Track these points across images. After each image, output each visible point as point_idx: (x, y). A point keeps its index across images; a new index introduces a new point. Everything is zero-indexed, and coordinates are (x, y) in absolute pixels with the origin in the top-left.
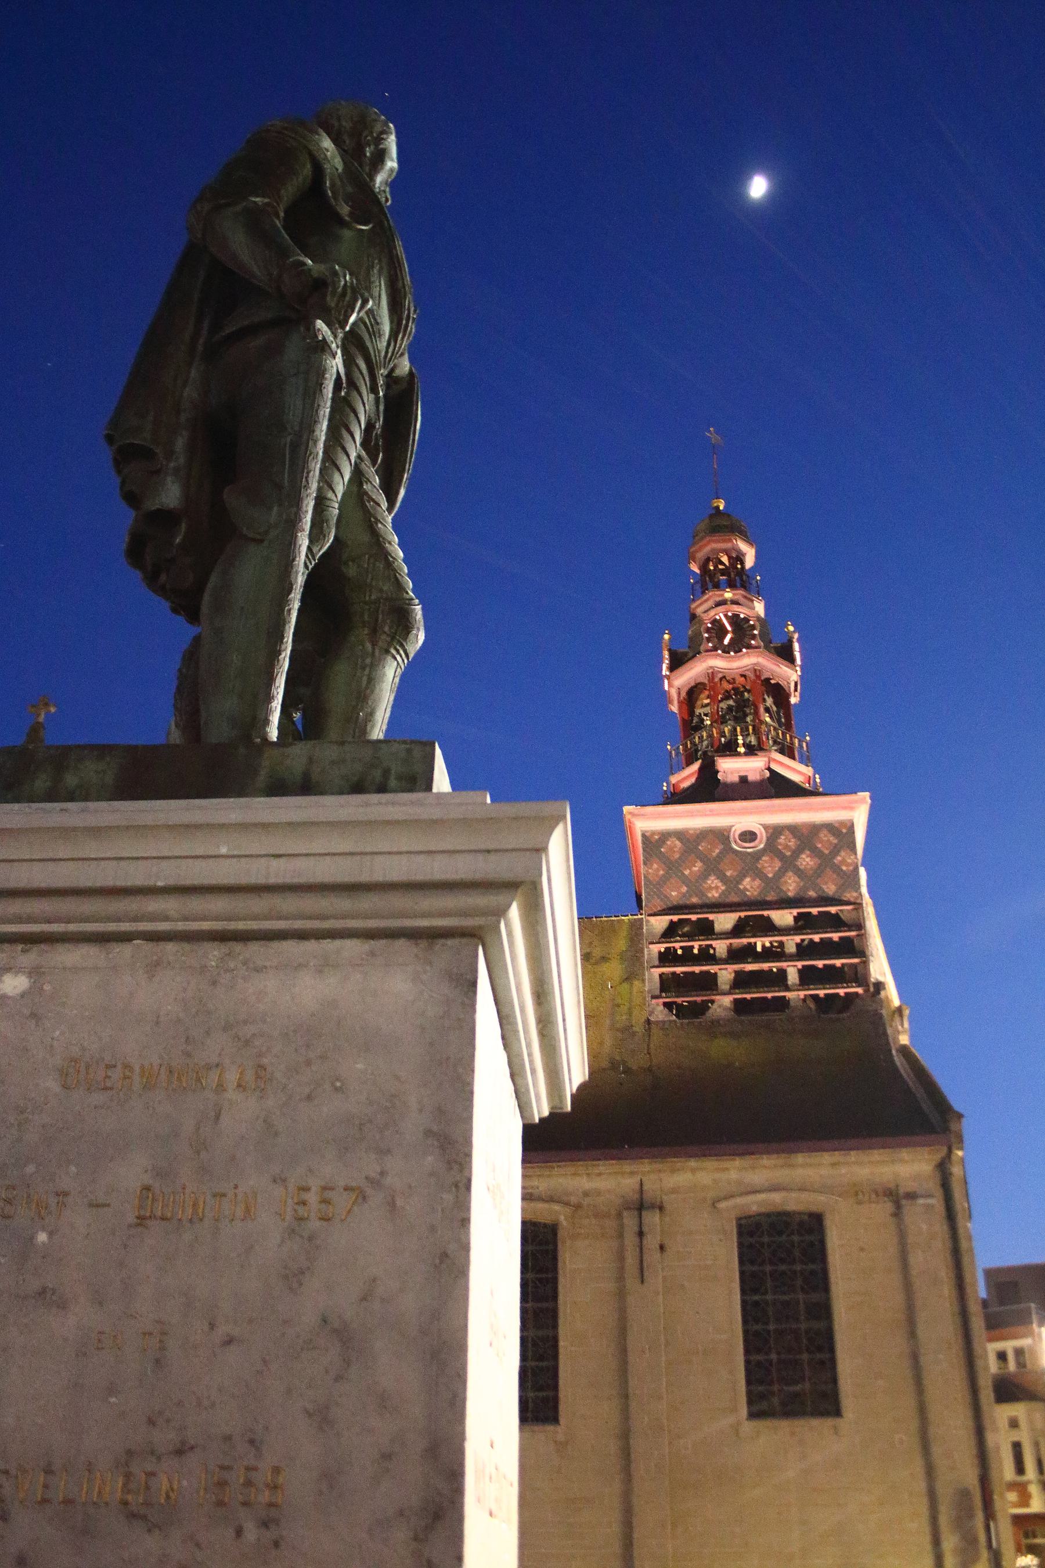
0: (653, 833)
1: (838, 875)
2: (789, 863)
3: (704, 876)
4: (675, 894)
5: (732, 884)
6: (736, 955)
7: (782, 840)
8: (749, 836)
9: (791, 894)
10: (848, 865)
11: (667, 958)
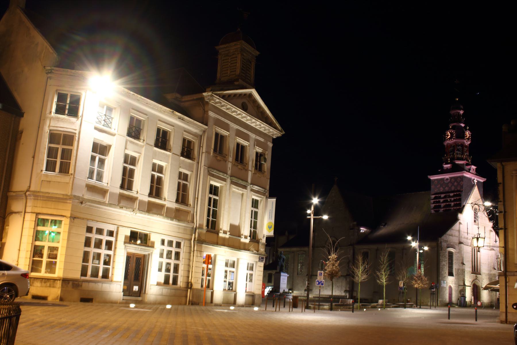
4: (436, 191)
6: (443, 202)
7: (452, 180)
8: (447, 179)
11: (434, 203)
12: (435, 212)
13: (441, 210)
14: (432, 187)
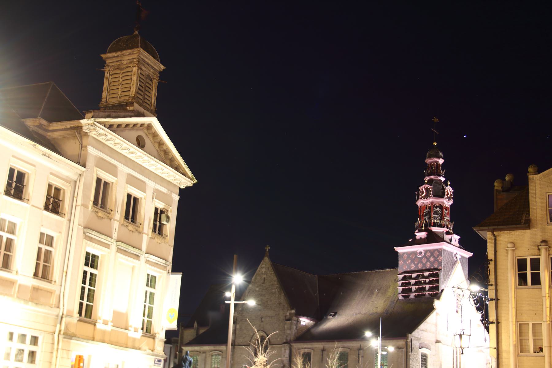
0: (401, 253)
1: (438, 262)
2: (428, 260)
3: (411, 263)
4: (405, 268)
5: (416, 265)
6: (416, 284)
8: (421, 253)
9: (428, 268)
10: (440, 260)
11: (402, 285)
12: (403, 298)
13: (412, 296)
14: (400, 263)
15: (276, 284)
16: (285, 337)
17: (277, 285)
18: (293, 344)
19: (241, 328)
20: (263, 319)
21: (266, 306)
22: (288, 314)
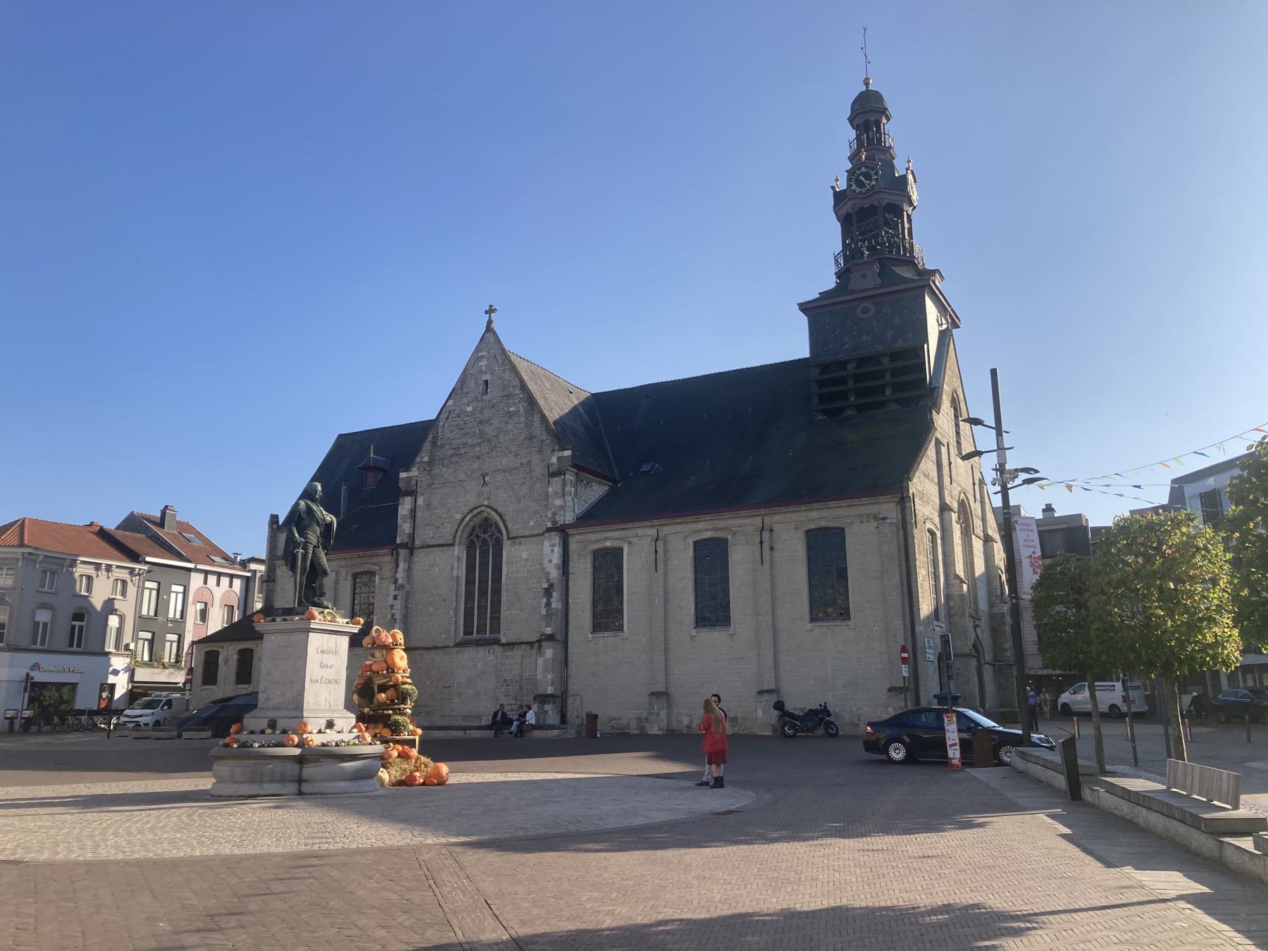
15: (518, 392)
16: (550, 515)
17: (521, 396)
18: (570, 531)
19: (428, 505)
20: (487, 479)
21: (495, 446)
22: (554, 460)
